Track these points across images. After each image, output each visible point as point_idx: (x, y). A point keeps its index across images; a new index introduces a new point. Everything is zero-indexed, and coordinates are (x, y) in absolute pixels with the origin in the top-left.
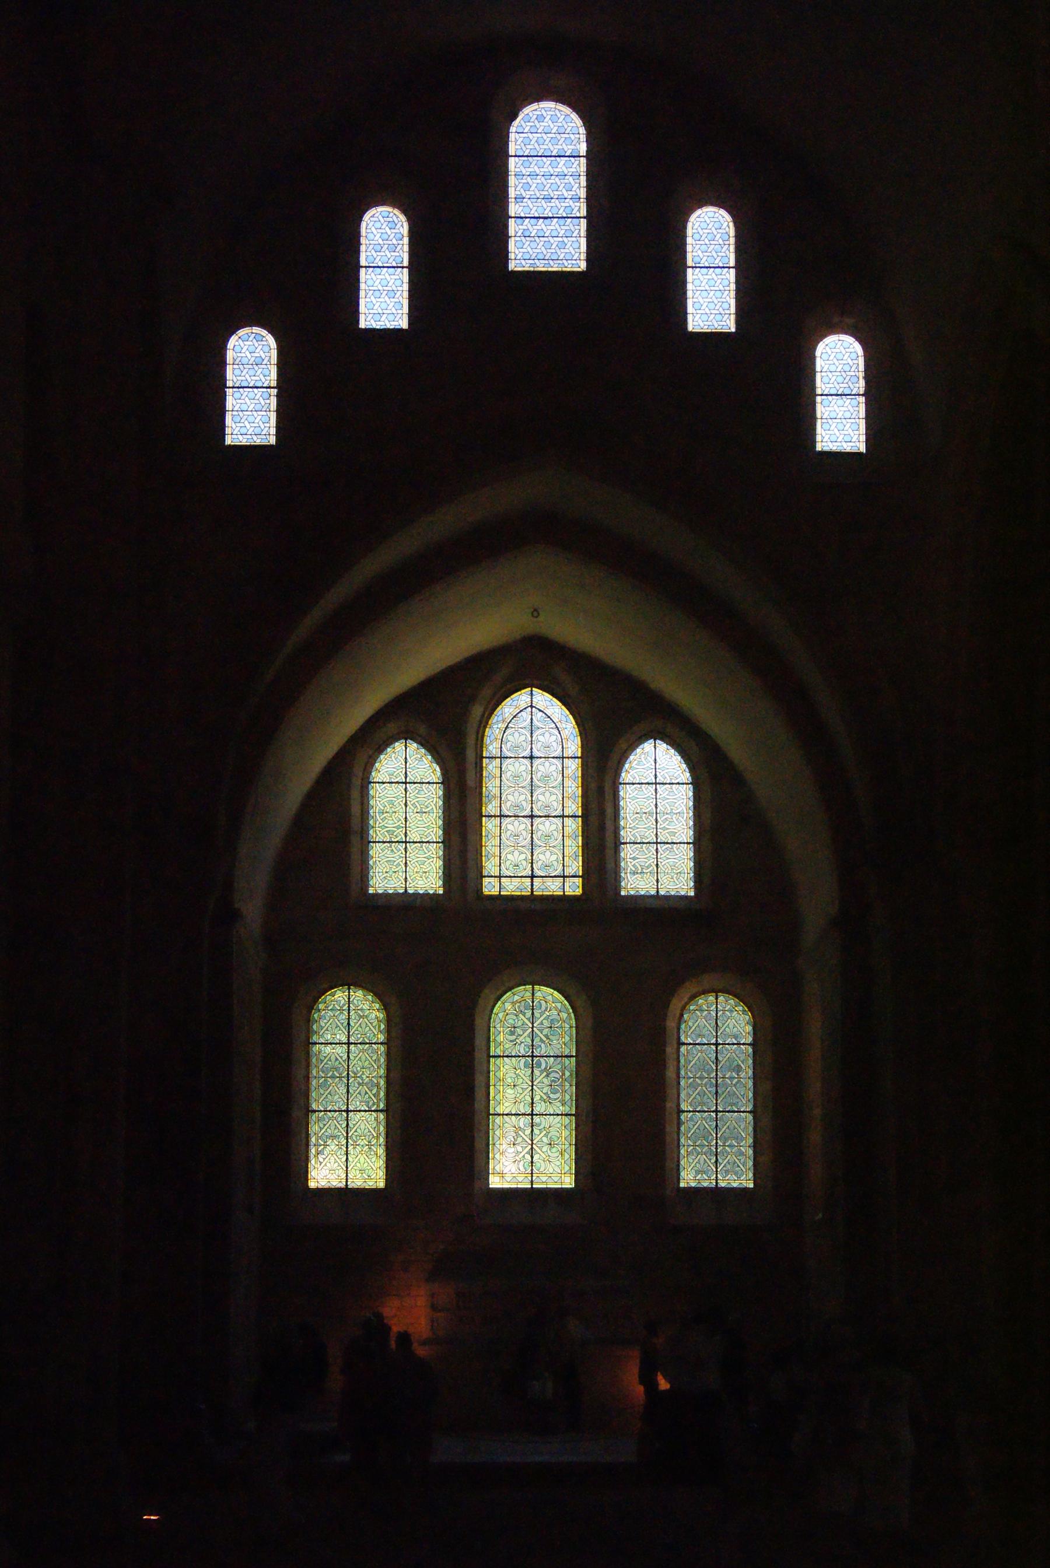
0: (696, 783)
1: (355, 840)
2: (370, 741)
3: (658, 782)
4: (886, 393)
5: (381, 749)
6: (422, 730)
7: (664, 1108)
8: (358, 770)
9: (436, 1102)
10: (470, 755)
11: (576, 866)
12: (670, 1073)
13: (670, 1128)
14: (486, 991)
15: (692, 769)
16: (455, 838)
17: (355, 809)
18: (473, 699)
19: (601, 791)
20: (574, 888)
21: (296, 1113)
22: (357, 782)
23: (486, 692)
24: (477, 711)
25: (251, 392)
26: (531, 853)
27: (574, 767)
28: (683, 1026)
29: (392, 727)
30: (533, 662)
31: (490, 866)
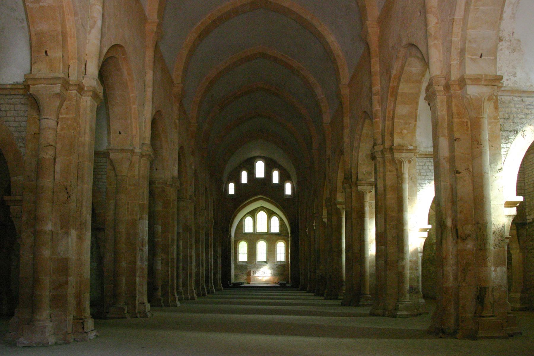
4: (293, 189)
9: (252, 252)
20: (266, 231)
26: (262, 228)
30: (262, 208)
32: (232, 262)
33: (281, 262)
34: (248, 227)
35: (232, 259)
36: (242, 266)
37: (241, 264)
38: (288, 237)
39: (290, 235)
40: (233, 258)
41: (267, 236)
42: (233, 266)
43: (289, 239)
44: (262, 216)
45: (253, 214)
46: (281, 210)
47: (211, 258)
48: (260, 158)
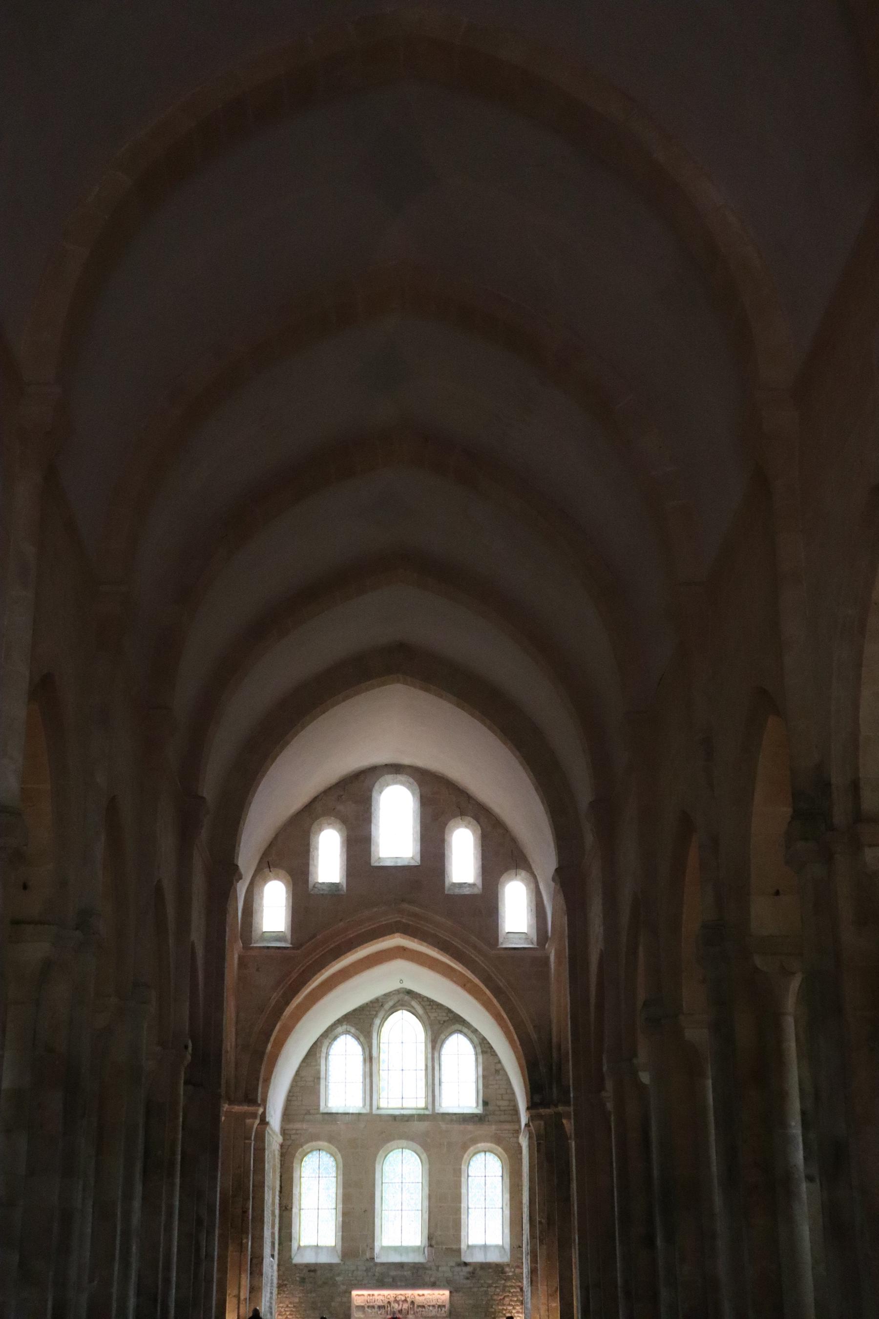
0: (476, 1054)
1: (322, 1082)
2: (329, 1035)
3: (459, 1052)
5: (335, 1038)
6: (353, 1030)
7: (460, 1207)
8: (324, 1050)
10: (375, 1042)
11: (422, 1092)
12: (464, 1191)
13: (463, 1217)
14: (381, 1152)
15: (475, 1047)
16: (368, 1080)
17: (323, 1068)
18: (376, 1016)
19: (433, 1059)
20: (422, 1104)
21: (295, 1210)
22: (323, 1055)
23: (381, 1014)
24: (377, 1021)
25: (273, 909)
27: (422, 1047)
28: (470, 1168)
29: (340, 1029)
31: (383, 1094)
32: (267, 1251)
33: (485, 1247)
34: (343, 1087)
35: (267, 1233)
36: (312, 1269)
37: (308, 1258)
38: (517, 1132)
39: (524, 1118)
40: (270, 1231)
41: (423, 1126)
42: (270, 1266)
43: (524, 1142)
44: (402, 1031)
45: (363, 1022)
46: (487, 1005)
47: (168, 1229)
48: (396, 769)
